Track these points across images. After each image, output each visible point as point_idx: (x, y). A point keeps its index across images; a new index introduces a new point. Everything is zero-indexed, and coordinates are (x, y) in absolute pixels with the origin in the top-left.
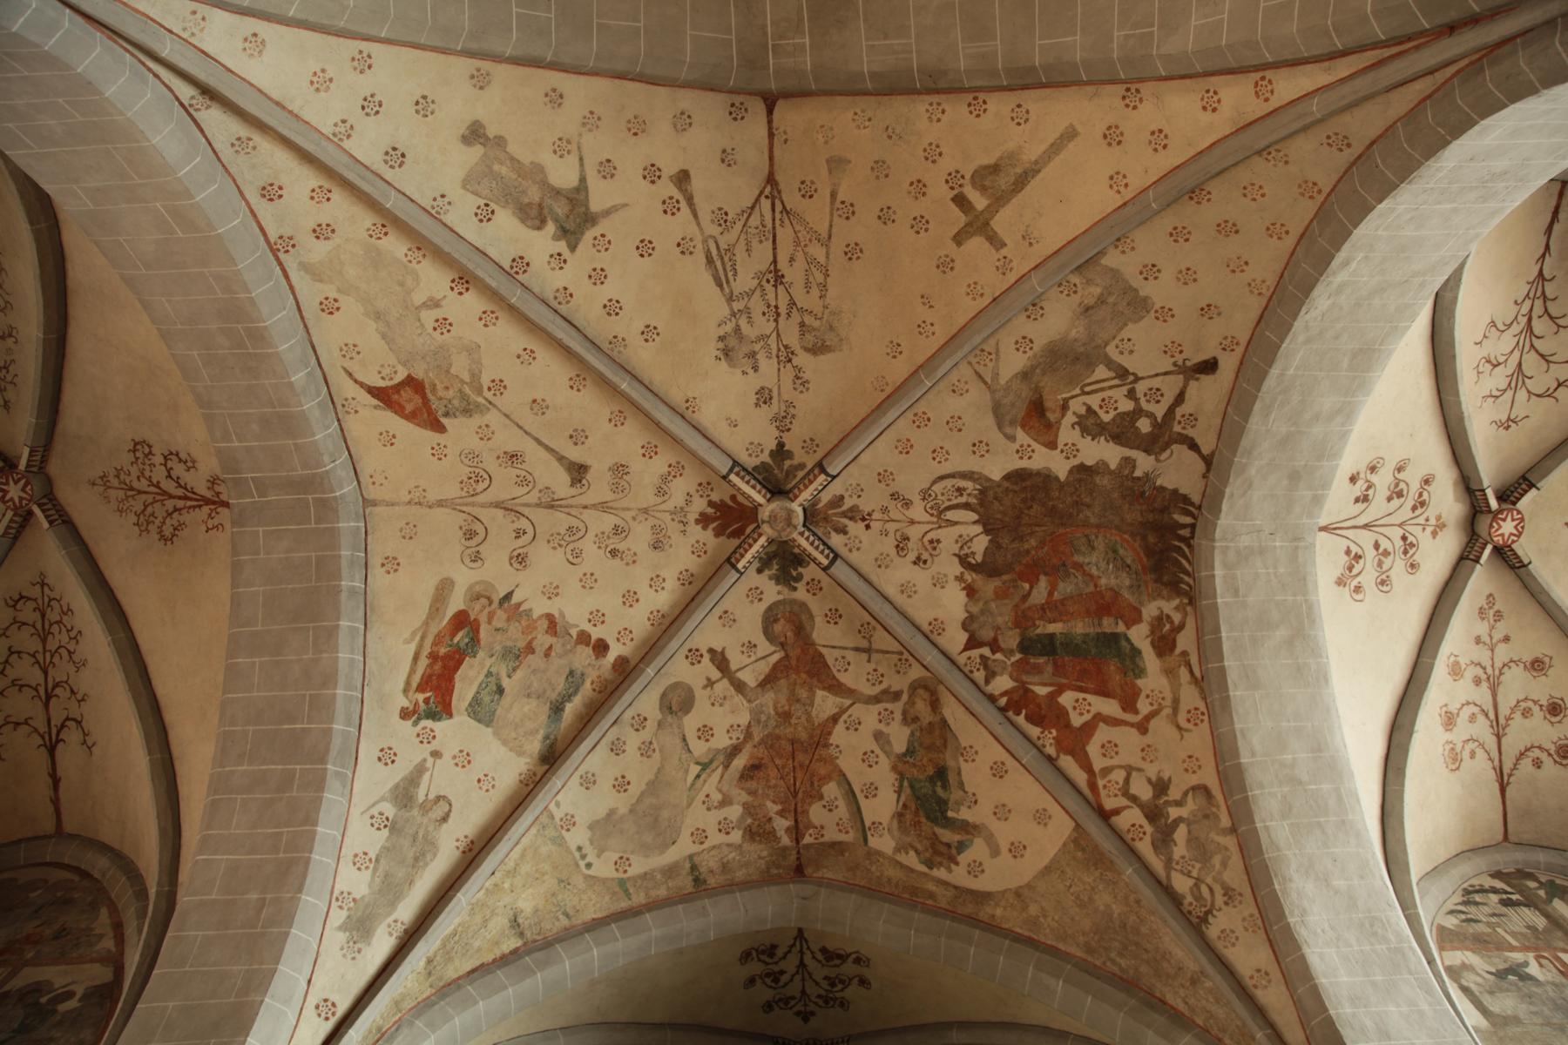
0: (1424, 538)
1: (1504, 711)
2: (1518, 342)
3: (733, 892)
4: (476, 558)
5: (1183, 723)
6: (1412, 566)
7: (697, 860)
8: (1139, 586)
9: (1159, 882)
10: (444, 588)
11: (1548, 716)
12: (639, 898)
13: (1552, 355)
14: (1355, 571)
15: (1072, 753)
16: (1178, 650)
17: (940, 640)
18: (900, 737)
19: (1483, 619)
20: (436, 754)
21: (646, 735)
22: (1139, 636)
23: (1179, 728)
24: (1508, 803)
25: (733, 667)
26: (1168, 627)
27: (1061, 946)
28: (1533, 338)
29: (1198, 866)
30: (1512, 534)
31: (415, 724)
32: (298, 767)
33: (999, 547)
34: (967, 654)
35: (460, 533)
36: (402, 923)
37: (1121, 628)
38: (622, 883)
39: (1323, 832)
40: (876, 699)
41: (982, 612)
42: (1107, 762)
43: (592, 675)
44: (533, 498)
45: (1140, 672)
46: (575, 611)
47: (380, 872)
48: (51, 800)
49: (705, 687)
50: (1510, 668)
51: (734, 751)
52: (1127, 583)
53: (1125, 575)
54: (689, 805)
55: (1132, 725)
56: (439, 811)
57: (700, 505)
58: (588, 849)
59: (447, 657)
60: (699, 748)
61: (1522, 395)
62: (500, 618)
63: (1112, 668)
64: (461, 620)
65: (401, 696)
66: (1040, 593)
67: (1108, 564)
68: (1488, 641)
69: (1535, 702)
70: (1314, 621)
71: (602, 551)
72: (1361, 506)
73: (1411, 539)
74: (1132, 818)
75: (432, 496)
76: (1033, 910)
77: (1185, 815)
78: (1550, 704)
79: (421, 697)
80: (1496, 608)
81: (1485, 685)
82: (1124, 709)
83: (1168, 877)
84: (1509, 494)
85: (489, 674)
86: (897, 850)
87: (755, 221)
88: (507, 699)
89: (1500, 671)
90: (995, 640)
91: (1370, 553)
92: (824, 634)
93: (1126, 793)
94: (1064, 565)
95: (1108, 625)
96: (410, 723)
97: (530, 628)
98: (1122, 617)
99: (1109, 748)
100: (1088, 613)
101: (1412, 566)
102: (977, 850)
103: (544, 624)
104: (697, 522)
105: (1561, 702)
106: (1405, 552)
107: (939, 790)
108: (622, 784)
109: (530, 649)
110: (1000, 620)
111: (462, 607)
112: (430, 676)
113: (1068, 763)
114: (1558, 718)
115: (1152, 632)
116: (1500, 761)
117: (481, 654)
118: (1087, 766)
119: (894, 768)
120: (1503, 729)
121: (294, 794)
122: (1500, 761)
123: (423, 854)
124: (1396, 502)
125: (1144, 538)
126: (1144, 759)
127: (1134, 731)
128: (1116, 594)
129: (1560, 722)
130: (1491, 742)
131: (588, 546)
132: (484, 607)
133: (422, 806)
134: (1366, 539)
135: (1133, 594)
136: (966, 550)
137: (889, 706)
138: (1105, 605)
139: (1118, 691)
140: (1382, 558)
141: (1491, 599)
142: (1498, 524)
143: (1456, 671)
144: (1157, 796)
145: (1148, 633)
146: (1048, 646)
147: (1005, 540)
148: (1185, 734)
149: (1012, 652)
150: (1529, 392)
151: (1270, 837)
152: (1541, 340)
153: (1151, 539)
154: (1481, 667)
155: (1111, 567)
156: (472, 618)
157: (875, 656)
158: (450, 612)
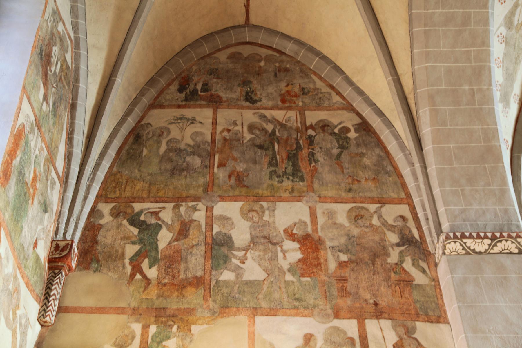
32: (472, 10)
36: (518, 96)
47: (505, 69)
48: (245, 5)
121: (472, 27)
123: (519, 56)
133: (516, 27)
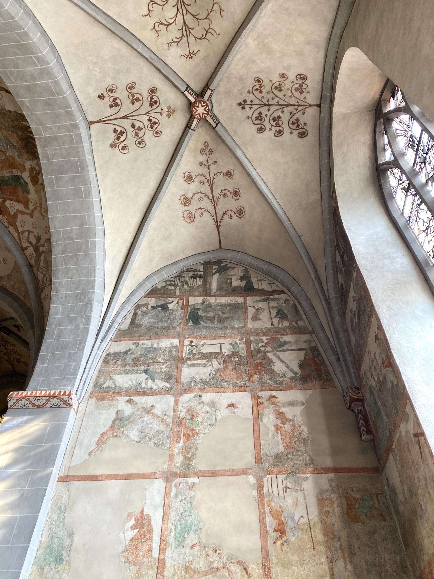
0: (163, 119)
1: (216, 195)
2: (178, 10)
5: (44, 214)
6: (157, 133)
8: (21, 155)
9: (35, 276)
11: (234, 197)
13: (198, 15)
14: (122, 139)
15: (11, 225)
16: (39, 183)
19: (204, 154)
22: (26, 176)
23: (42, 215)
24: (220, 233)
26: (35, 173)
27: (19, 296)
28: (186, 6)
29: (45, 270)
30: (203, 113)
37: (19, 174)
39: (77, 259)
45: (28, 192)
50: (217, 176)
53: (15, 150)
55: (28, 214)
61: (192, 39)
63: (19, 190)
67: (7, 146)
68: (206, 164)
69: (228, 191)
70: (83, 168)
72: (114, 110)
73: (154, 120)
74: (31, 250)
76: (12, 283)
77: (44, 250)
78: (234, 192)
80: (209, 148)
81: (206, 184)
82: (25, 208)
83: (37, 274)
84: (201, 95)
89: (213, 177)
91: (130, 130)
95: (16, 172)
98: (18, 169)
99: (23, 223)
101: (157, 133)
105: (238, 190)
106: (152, 127)
113: (11, 229)
114: (237, 198)
115: (30, 175)
116: (216, 216)
118: (17, 230)
120: (217, 203)
122: (216, 216)
124: (137, 105)
125: (17, 133)
126: (33, 228)
128: (14, 159)
129: (238, 199)
130: (212, 209)
134: (127, 123)
135: (20, 158)
140: (137, 131)
141: (206, 144)
142: (195, 109)
143: (189, 179)
145: (29, 175)
150: (195, 37)
151: (55, 261)
152: (190, 6)
153: (20, 133)
154: (204, 176)
155: (9, 146)
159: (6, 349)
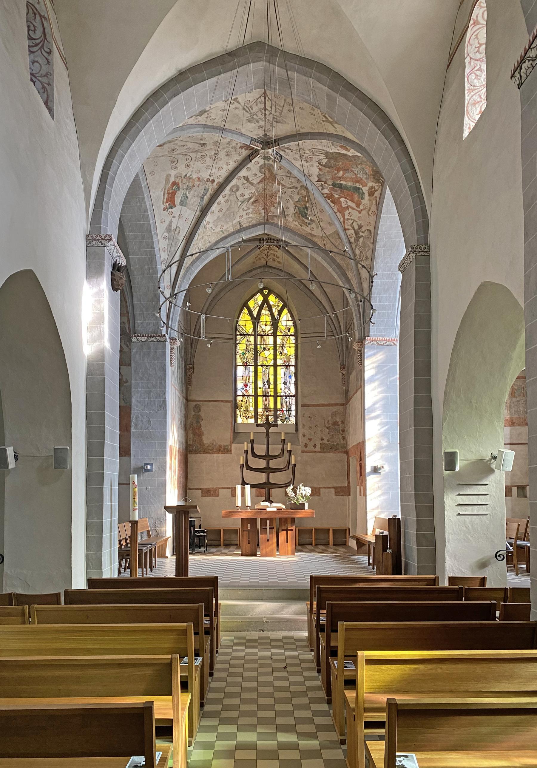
3: (250, 228)
4: (176, 168)
5: (370, 214)
7: (241, 222)
10: (168, 176)
12: (226, 233)
16: (374, 196)
17: (311, 178)
18: (296, 198)
20: (174, 217)
21: (226, 198)
22: (365, 189)
23: (369, 215)
25: (250, 180)
26: (373, 189)
29: (362, 248)
31: (167, 211)
33: (330, 162)
34: (317, 182)
35: (170, 162)
37: (361, 187)
38: (222, 231)
40: (290, 188)
41: (323, 175)
42: (349, 217)
43: (210, 188)
44: (191, 150)
45: (363, 198)
46: (205, 175)
49: (242, 185)
51: (250, 198)
52: (365, 177)
54: (238, 211)
55: (357, 210)
56: (177, 231)
57: (239, 145)
58: (213, 227)
59: (172, 192)
60: (241, 199)
62: (185, 180)
64: (174, 183)
65: (163, 205)
66: (341, 174)
71: (211, 160)
74: (352, 232)
75: (160, 155)
79: (167, 204)
82: (356, 206)
83: (355, 249)
85: (183, 194)
86: (293, 221)
87: (259, 100)
88: (189, 199)
90: (326, 181)
92: (276, 172)
93: (352, 225)
94: (348, 170)
95: (357, 185)
96: (166, 211)
97: (194, 180)
100: (353, 181)
102: (313, 225)
103: (197, 179)
104: (239, 148)
107: (305, 211)
108: (221, 210)
109: (194, 186)
110: (328, 178)
111: (174, 180)
112: (168, 198)
113: (338, 214)
117: (181, 190)
119: (294, 204)
127: (357, 212)
131: (208, 159)
132: (180, 179)
133: (173, 231)
136: (320, 161)
137: (294, 190)
138: (358, 181)
139: (356, 201)
144: (359, 229)
146: (340, 186)
147: (332, 161)
148: (370, 217)
149: (330, 185)
156: (177, 182)
157: (291, 178)
158: (171, 182)
159: (268, 253)
